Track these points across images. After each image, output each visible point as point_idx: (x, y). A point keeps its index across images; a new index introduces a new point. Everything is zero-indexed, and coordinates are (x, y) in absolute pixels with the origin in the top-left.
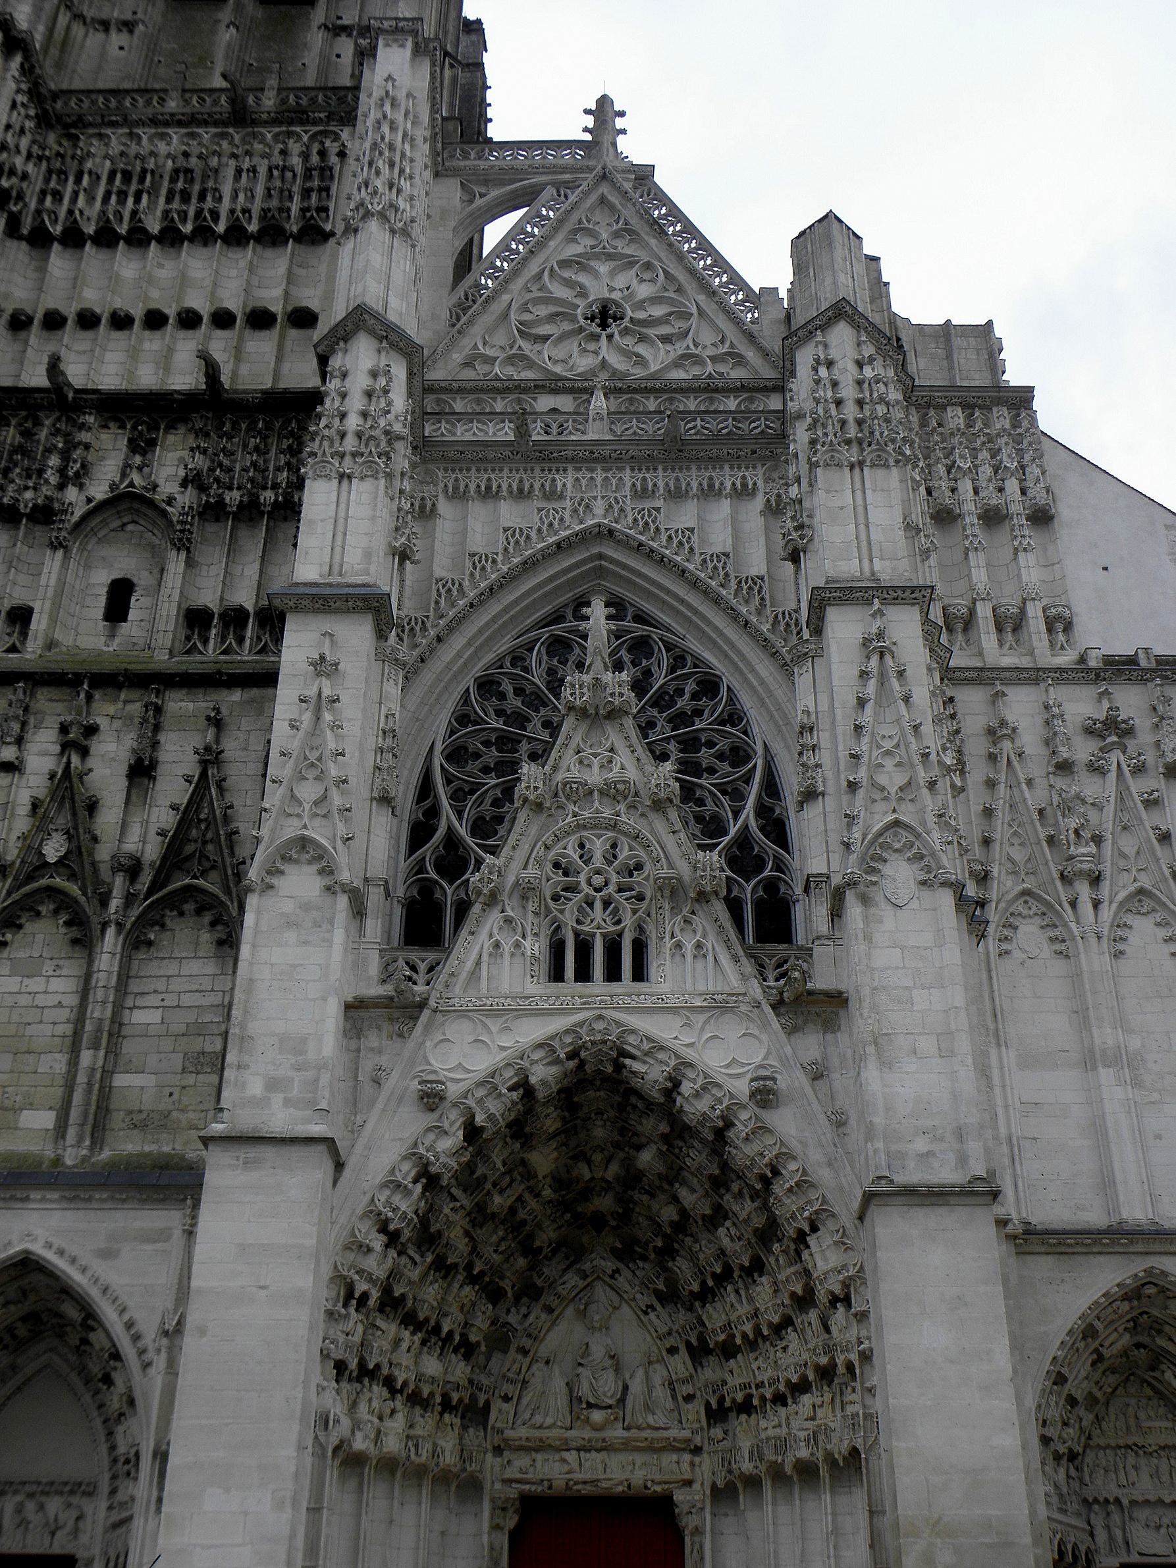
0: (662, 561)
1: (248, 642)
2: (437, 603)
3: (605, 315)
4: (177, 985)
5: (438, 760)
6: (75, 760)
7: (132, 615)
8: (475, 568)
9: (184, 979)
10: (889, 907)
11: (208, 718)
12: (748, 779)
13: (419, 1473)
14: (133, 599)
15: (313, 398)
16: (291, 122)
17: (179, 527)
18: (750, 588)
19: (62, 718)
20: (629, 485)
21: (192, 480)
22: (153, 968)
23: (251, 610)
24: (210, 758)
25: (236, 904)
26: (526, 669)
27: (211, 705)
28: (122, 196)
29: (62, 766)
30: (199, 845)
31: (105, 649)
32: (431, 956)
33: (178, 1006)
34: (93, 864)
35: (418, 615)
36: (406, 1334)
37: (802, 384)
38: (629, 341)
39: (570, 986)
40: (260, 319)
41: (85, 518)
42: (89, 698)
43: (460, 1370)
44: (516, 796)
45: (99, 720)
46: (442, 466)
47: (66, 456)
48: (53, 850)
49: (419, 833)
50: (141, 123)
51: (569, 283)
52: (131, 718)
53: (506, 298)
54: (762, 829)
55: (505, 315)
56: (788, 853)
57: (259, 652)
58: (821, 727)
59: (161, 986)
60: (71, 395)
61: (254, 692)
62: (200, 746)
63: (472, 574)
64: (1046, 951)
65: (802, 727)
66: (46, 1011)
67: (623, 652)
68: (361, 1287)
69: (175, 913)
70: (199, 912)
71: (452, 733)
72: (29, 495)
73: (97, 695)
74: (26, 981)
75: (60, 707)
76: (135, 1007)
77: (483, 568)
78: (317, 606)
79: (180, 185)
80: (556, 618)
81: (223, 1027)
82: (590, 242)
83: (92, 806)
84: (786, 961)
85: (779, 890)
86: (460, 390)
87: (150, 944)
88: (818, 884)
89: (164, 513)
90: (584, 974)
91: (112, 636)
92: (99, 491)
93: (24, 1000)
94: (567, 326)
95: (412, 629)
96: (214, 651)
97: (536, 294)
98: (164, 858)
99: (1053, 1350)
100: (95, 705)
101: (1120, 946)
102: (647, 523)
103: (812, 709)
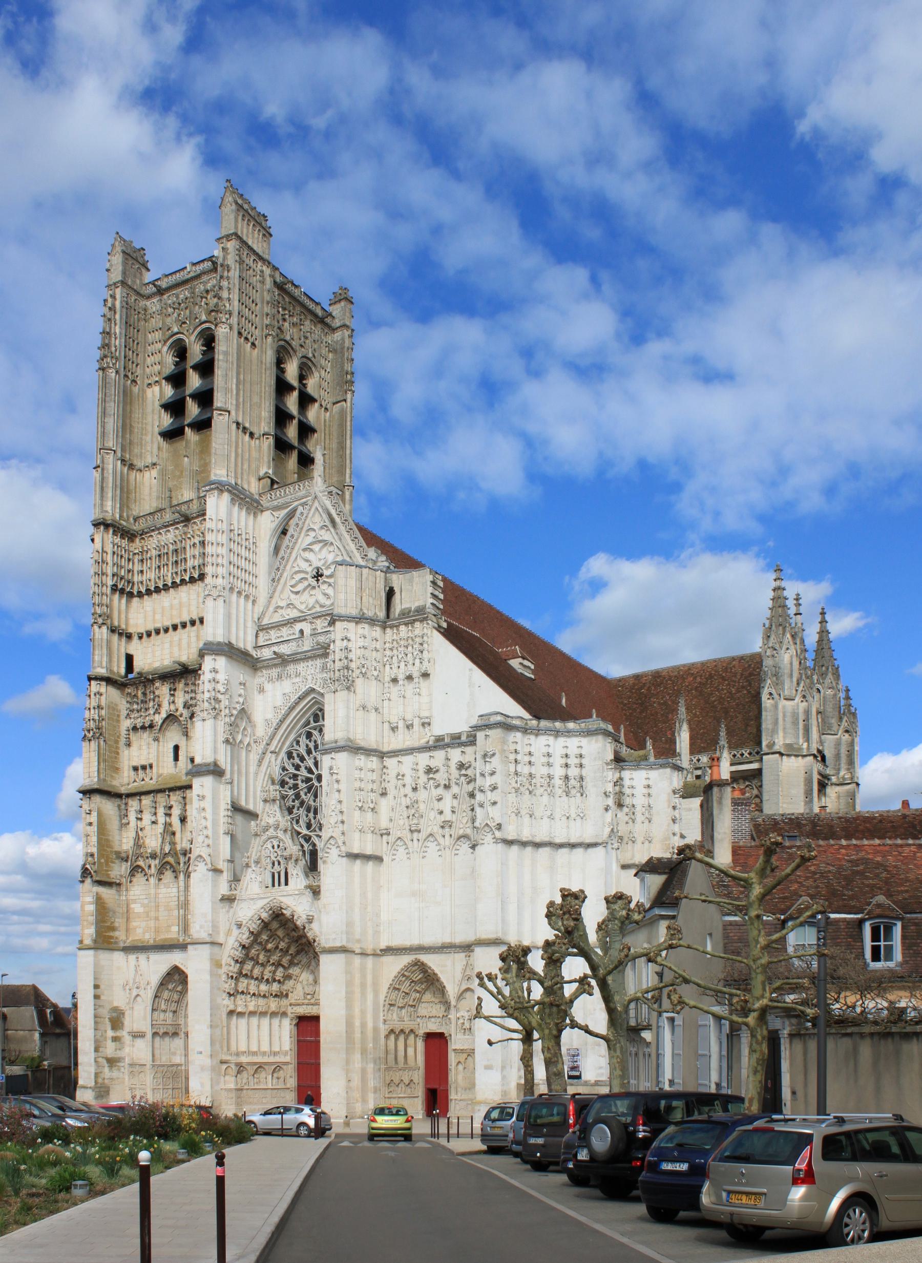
3: (318, 576)
6: (168, 819)
7: (180, 758)
13: (263, 1014)
21: (186, 706)
28: (159, 567)
36: (253, 981)
38: (324, 587)
41: (161, 726)
42: (169, 796)
43: (275, 987)
45: (172, 803)
47: (154, 701)
48: (167, 849)
51: (307, 561)
53: (285, 574)
55: (286, 583)
60: (150, 677)
64: (406, 856)
68: (230, 974)
75: (163, 799)
79: (175, 559)
82: (312, 534)
83: (174, 834)
90: (273, 885)
92: (164, 715)
94: (306, 583)
97: (297, 569)
99: (390, 982)
100: (171, 797)
101: (425, 854)
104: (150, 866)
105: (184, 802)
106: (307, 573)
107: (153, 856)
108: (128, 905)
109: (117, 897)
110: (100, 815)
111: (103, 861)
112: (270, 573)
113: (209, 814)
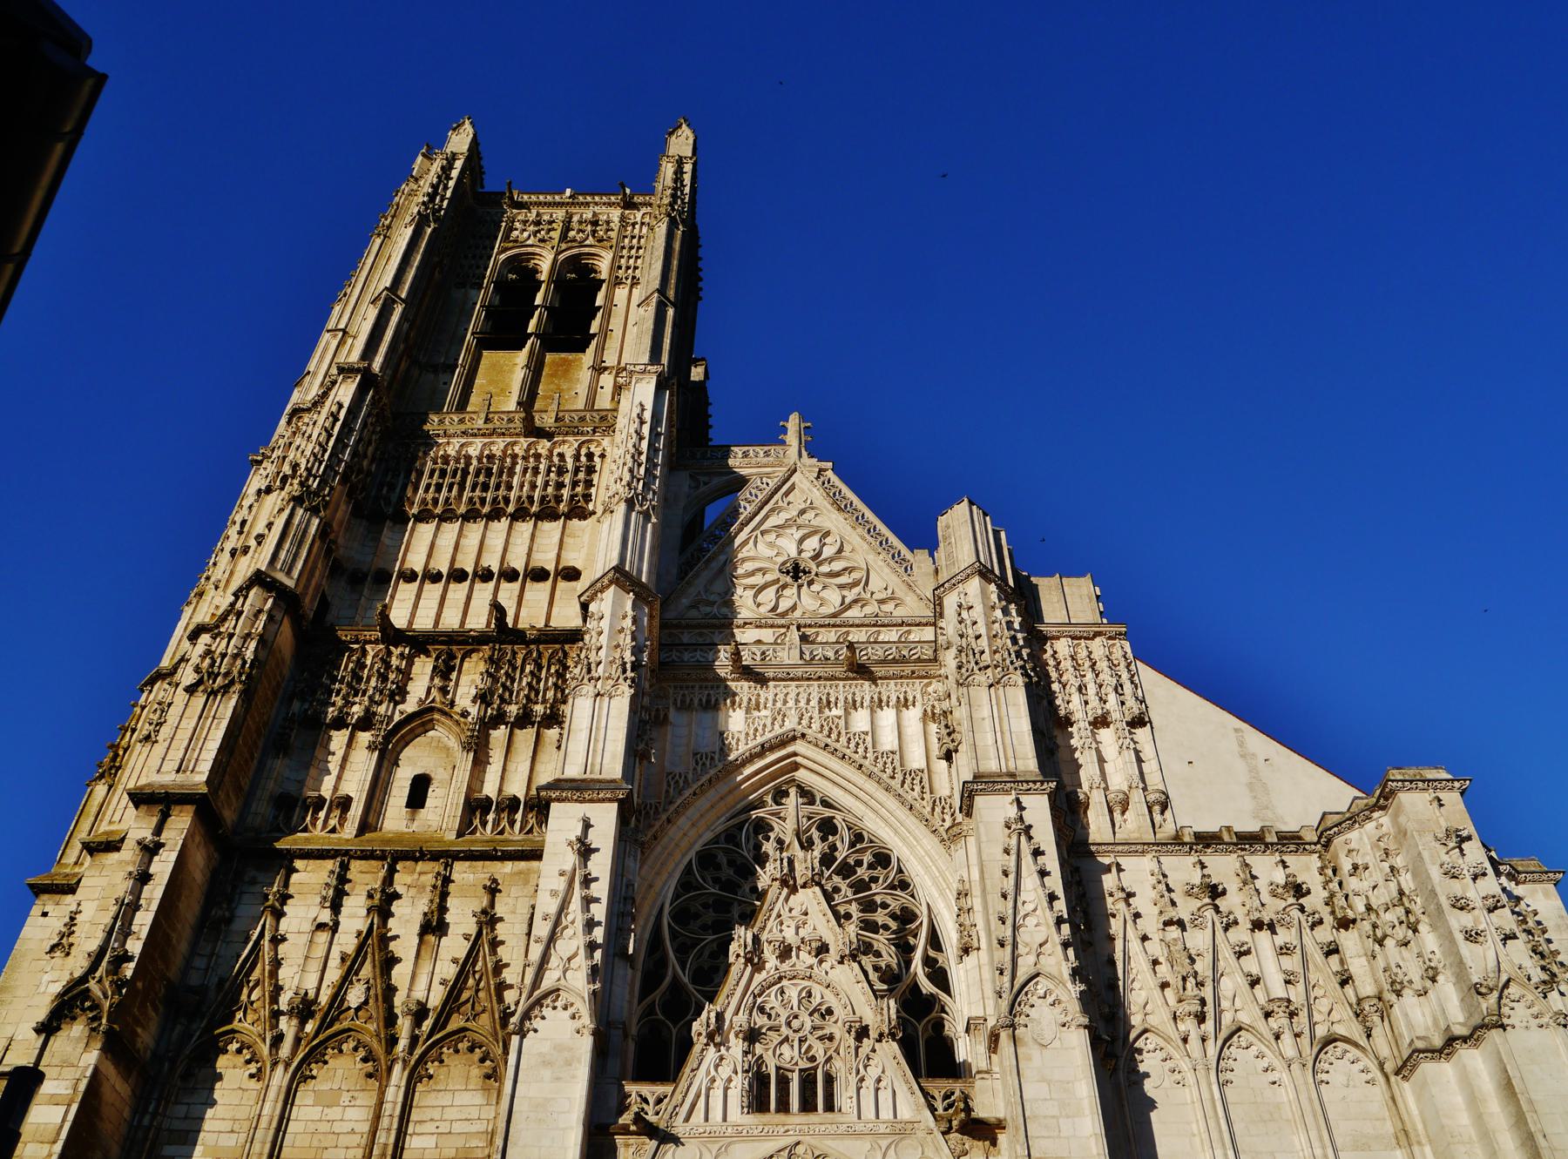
0: (844, 757)
1: (517, 826)
2: (667, 791)
3: (796, 571)
4: (451, 1114)
5: (666, 920)
7: (429, 802)
8: (697, 764)
9: (455, 1109)
10: (1036, 1047)
11: (485, 887)
14: (430, 790)
15: (575, 636)
16: (567, 434)
17: (469, 734)
18: (913, 779)
19: (369, 887)
20: (817, 699)
21: (483, 698)
22: (431, 1100)
23: (522, 800)
25: (501, 1044)
26: (738, 845)
27: (488, 876)
28: (439, 488)
29: (367, 926)
30: (473, 993)
31: (407, 830)
32: (660, 1089)
33: (450, 1133)
35: (653, 802)
37: (949, 624)
40: (539, 575)
42: (392, 871)
44: (731, 953)
45: (399, 889)
46: (672, 684)
48: (355, 996)
50: (453, 436)
52: (424, 887)
56: (950, 996)
57: (527, 833)
58: (974, 894)
59: (436, 1114)
61: (522, 865)
62: (479, 910)
63: (695, 769)
65: (959, 894)
66: (341, 1136)
67: (813, 829)
69: (451, 1050)
70: (471, 1050)
72: (355, 708)
74: (326, 1110)
76: (414, 1133)
77: (704, 764)
78: (575, 797)
79: (482, 479)
81: (486, 1152)
83: (390, 962)
84: (953, 1093)
85: (944, 1026)
86: (688, 627)
87: (430, 1077)
88: (976, 1025)
90: (783, 1107)
92: (410, 706)
93: (324, 1127)
95: (647, 813)
96: (492, 832)
98: (445, 1003)
102: (831, 729)
103: (966, 879)
104: (278, 1040)
106: (775, 563)
107: (304, 1008)
109: (126, 1113)
111: (139, 985)
112: (682, 550)
113: (601, 889)
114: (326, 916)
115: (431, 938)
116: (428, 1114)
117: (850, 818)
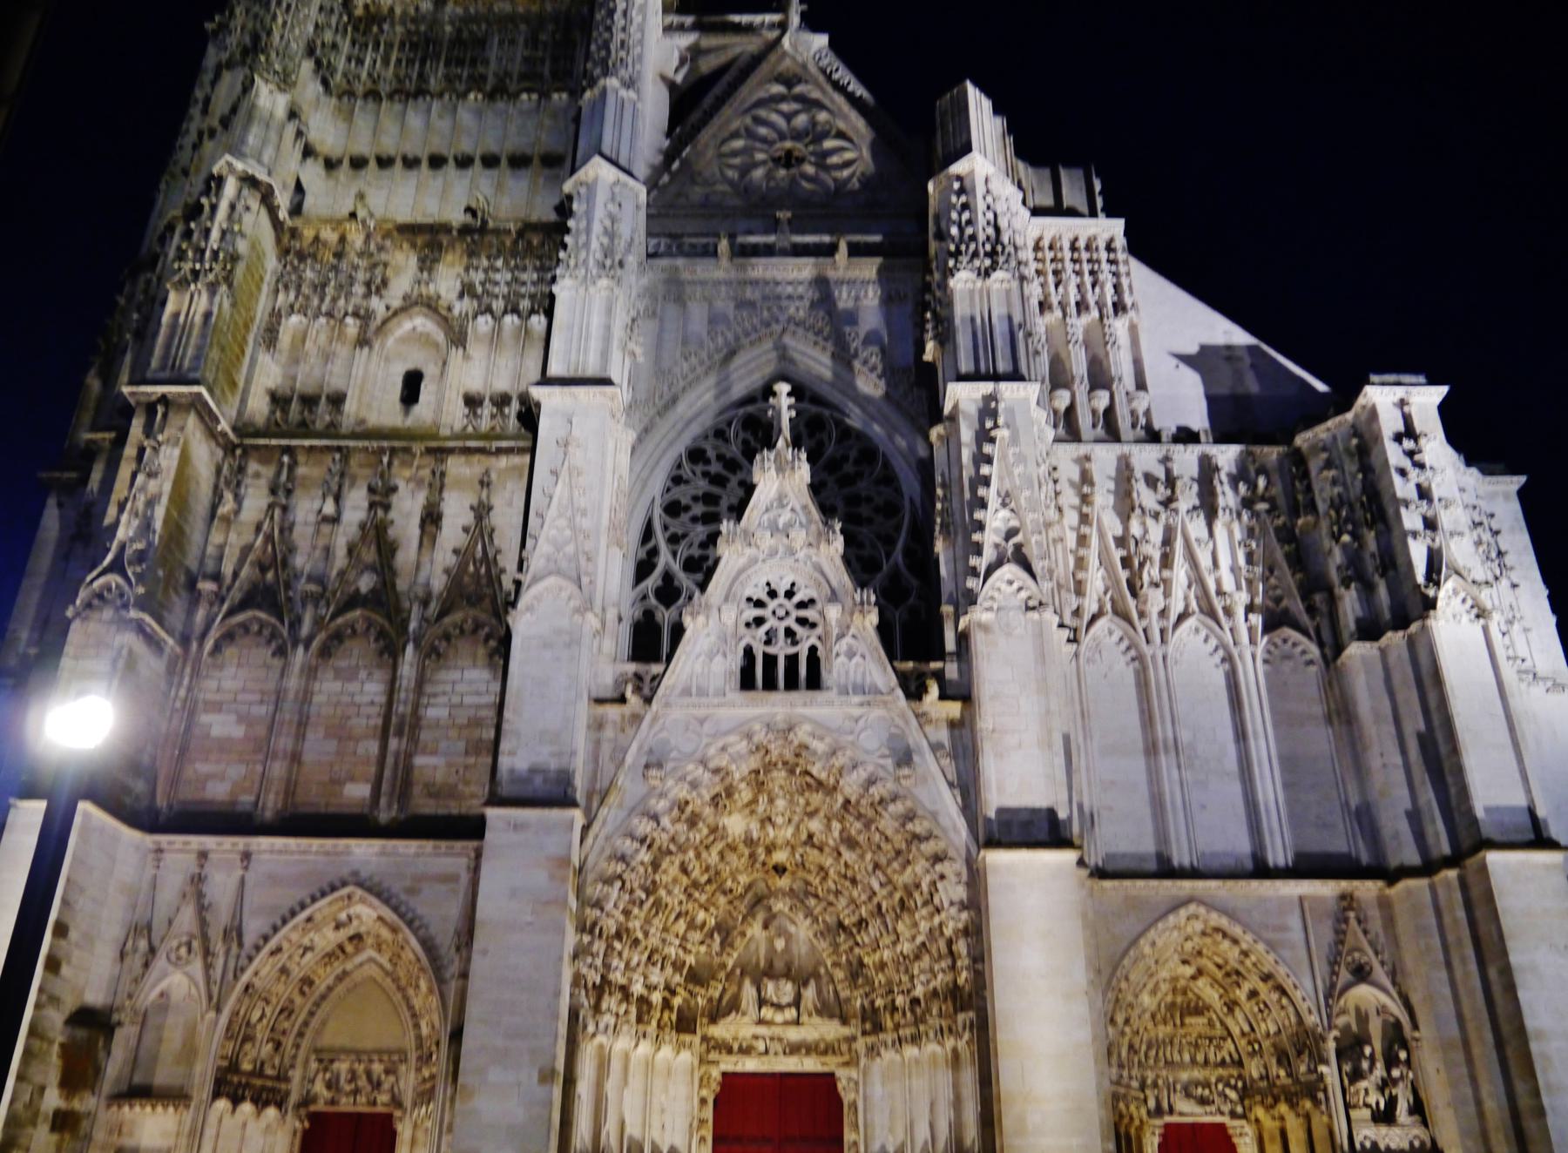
5: (658, 511)
6: (380, 513)
11: (482, 483)
12: (898, 528)
21: (467, 290)
22: (443, 675)
24: (482, 511)
34: (396, 595)
39: (759, 695)
42: (390, 464)
49: (643, 569)
54: (910, 567)
62: (475, 503)
71: (668, 490)
73: (396, 462)
80: (749, 400)
89: (446, 319)
91: (407, 412)
105: (438, 484)
108: (192, 713)
110: (185, 459)
114: (329, 508)
115: (430, 528)
116: (439, 688)
117: (836, 415)
